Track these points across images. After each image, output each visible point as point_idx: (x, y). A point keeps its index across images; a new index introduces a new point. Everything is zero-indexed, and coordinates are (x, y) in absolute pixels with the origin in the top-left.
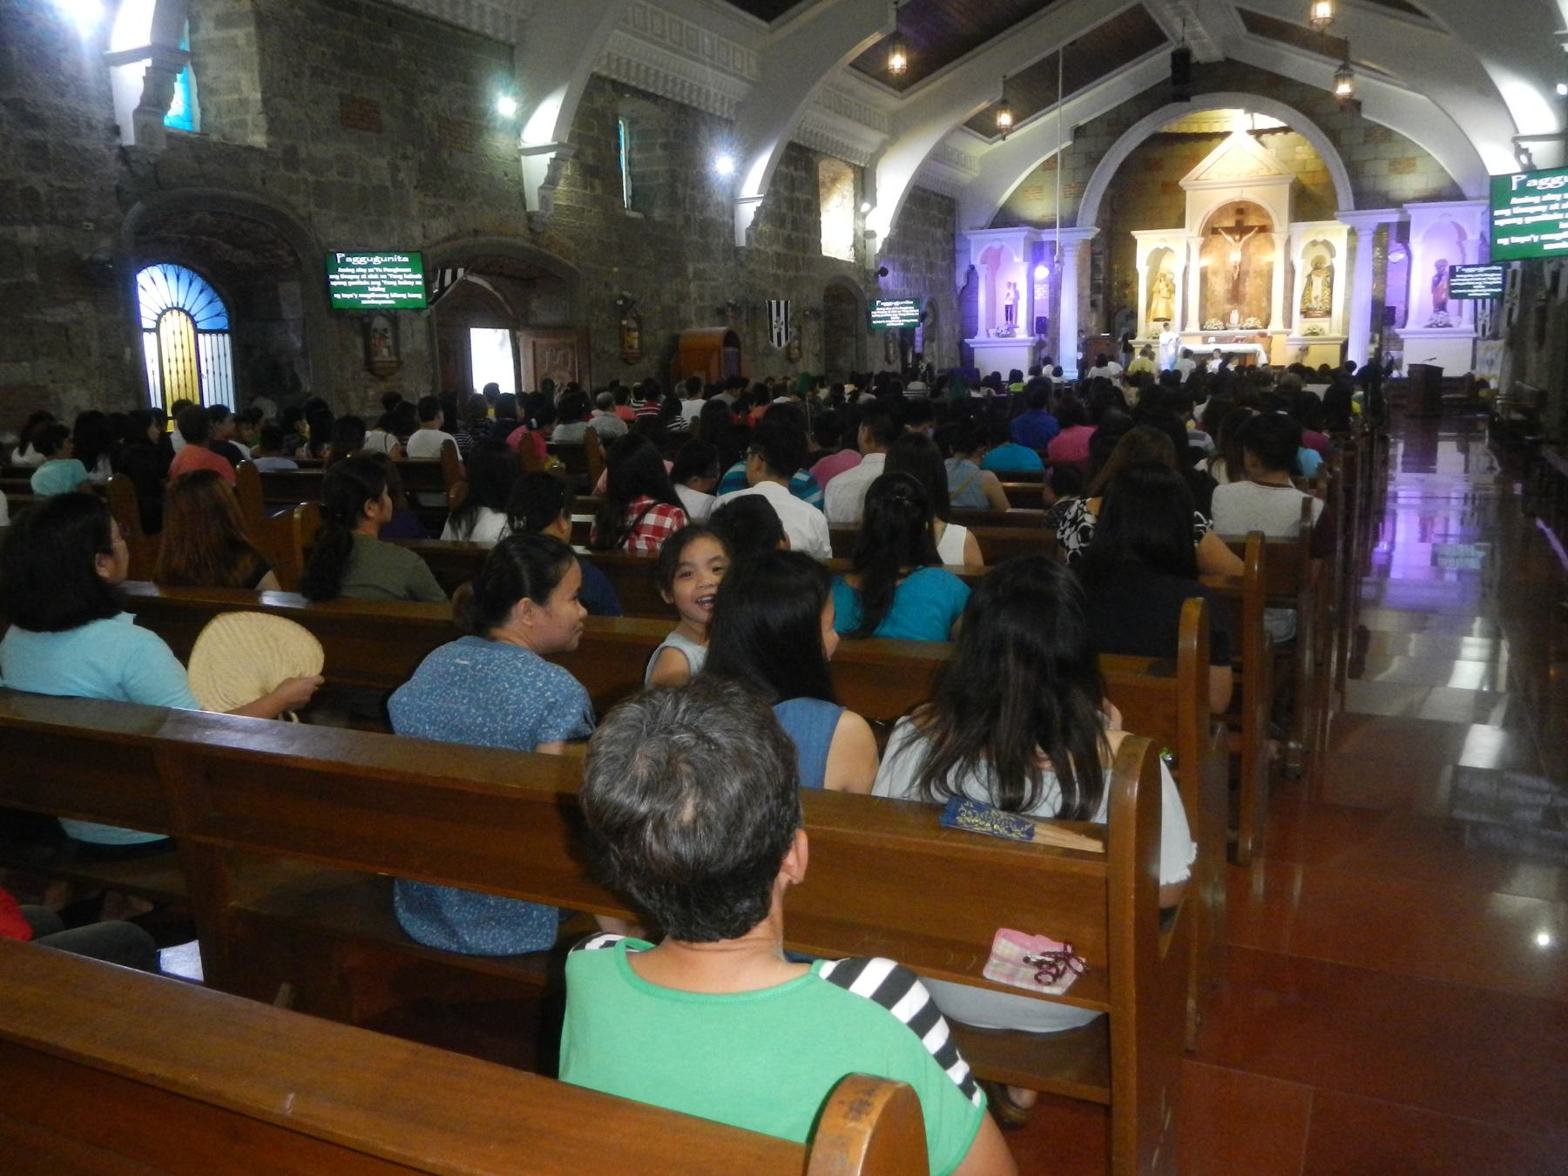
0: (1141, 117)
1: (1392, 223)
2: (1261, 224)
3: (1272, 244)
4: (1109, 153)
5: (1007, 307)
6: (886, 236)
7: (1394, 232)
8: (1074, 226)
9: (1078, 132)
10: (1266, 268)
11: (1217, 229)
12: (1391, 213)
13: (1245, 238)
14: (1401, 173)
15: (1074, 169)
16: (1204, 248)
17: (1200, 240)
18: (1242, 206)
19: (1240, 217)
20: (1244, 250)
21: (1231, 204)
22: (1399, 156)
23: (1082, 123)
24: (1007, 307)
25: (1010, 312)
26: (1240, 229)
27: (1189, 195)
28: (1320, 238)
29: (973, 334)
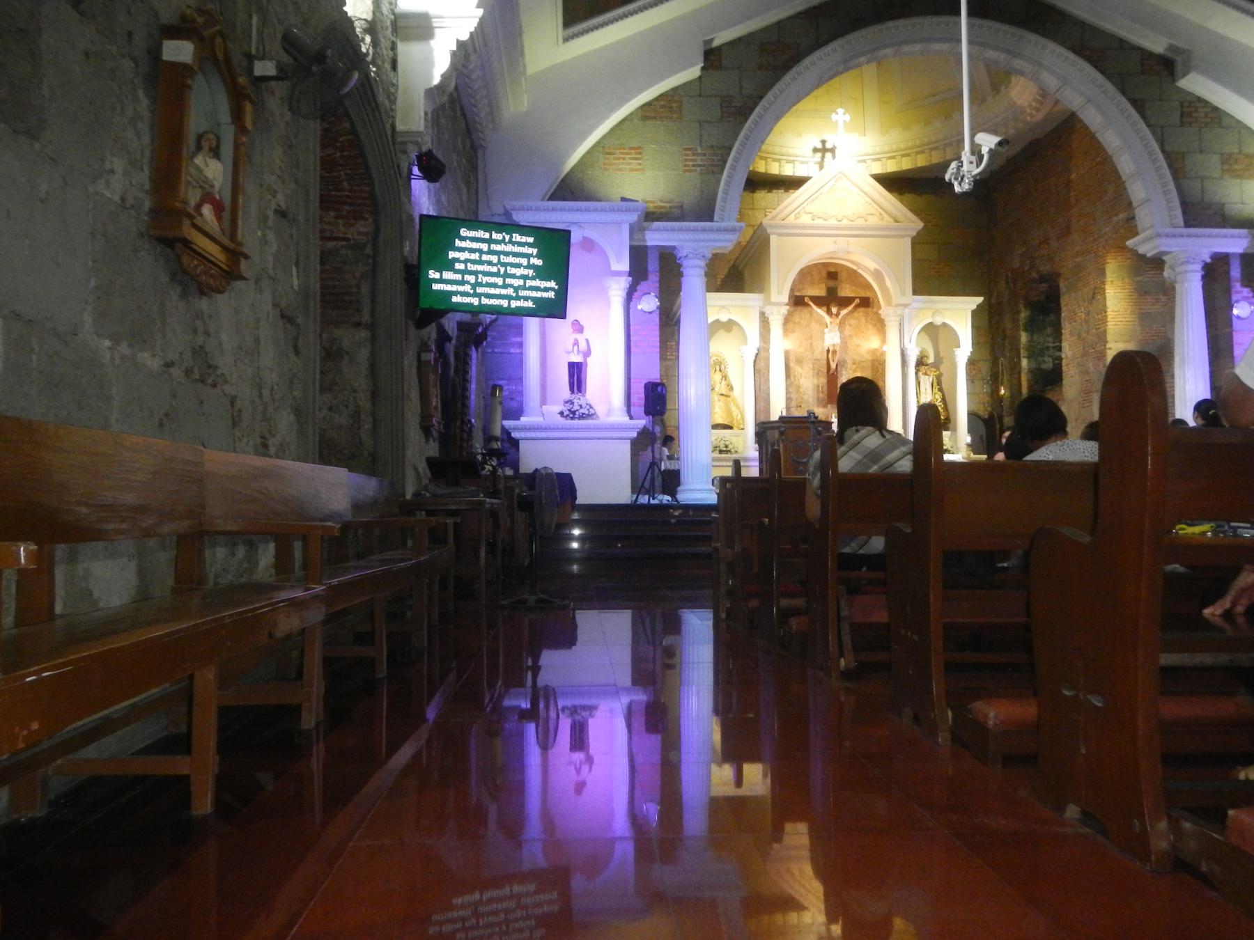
0: (819, 45)
1: (1234, 254)
2: (863, 295)
3: (880, 325)
4: (770, 96)
5: (572, 366)
6: (465, 37)
7: (1236, 272)
8: (712, 220)
9: (712, 57)
10: (869, 357)
11: (804, 297)
12: (1240, 237)
13: (844, 312)
14: (1240, 177)
15: (700, 122)
16: (787, 320)
17: (785, 310)
18: (832, 270)
19: (832, 283)
20: (841, 326)
21: (816, 265)
22: (1236, 151)
23: (721, 39)
24: (572, 366)
25: (577, 374)
26: (831, 300)
27: (773, 239)
28: (938, 321)
29: (517, 413)
